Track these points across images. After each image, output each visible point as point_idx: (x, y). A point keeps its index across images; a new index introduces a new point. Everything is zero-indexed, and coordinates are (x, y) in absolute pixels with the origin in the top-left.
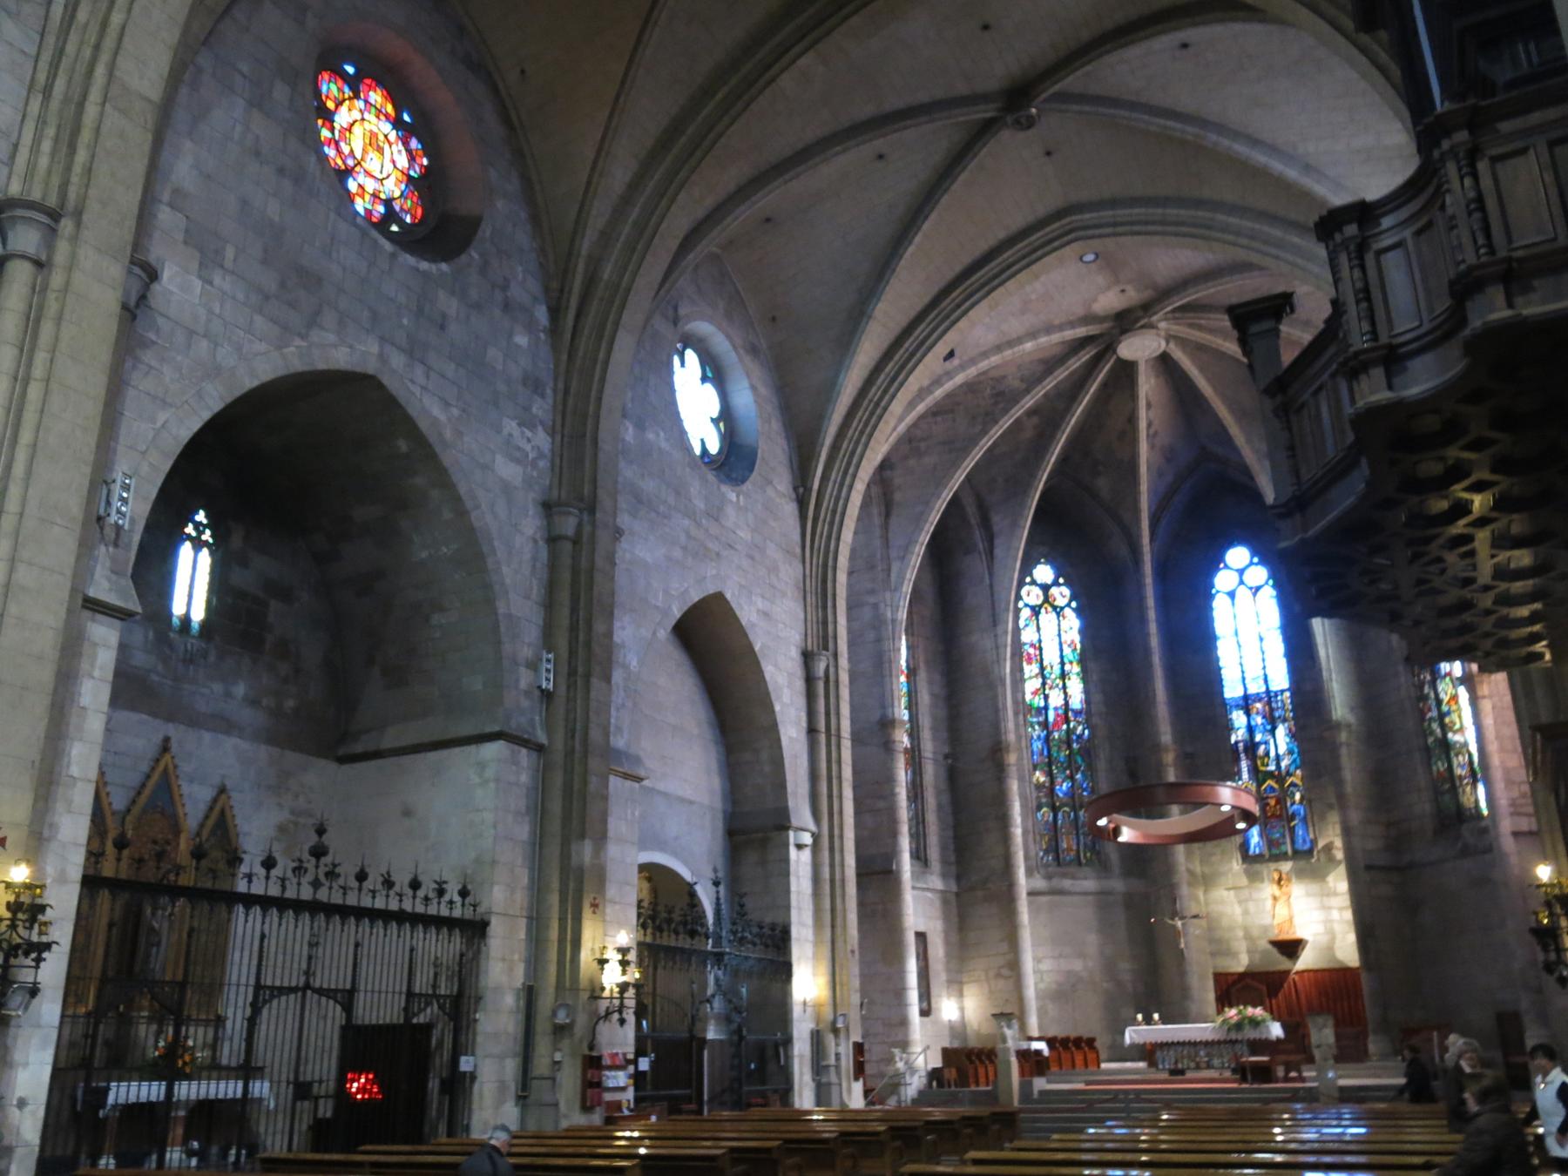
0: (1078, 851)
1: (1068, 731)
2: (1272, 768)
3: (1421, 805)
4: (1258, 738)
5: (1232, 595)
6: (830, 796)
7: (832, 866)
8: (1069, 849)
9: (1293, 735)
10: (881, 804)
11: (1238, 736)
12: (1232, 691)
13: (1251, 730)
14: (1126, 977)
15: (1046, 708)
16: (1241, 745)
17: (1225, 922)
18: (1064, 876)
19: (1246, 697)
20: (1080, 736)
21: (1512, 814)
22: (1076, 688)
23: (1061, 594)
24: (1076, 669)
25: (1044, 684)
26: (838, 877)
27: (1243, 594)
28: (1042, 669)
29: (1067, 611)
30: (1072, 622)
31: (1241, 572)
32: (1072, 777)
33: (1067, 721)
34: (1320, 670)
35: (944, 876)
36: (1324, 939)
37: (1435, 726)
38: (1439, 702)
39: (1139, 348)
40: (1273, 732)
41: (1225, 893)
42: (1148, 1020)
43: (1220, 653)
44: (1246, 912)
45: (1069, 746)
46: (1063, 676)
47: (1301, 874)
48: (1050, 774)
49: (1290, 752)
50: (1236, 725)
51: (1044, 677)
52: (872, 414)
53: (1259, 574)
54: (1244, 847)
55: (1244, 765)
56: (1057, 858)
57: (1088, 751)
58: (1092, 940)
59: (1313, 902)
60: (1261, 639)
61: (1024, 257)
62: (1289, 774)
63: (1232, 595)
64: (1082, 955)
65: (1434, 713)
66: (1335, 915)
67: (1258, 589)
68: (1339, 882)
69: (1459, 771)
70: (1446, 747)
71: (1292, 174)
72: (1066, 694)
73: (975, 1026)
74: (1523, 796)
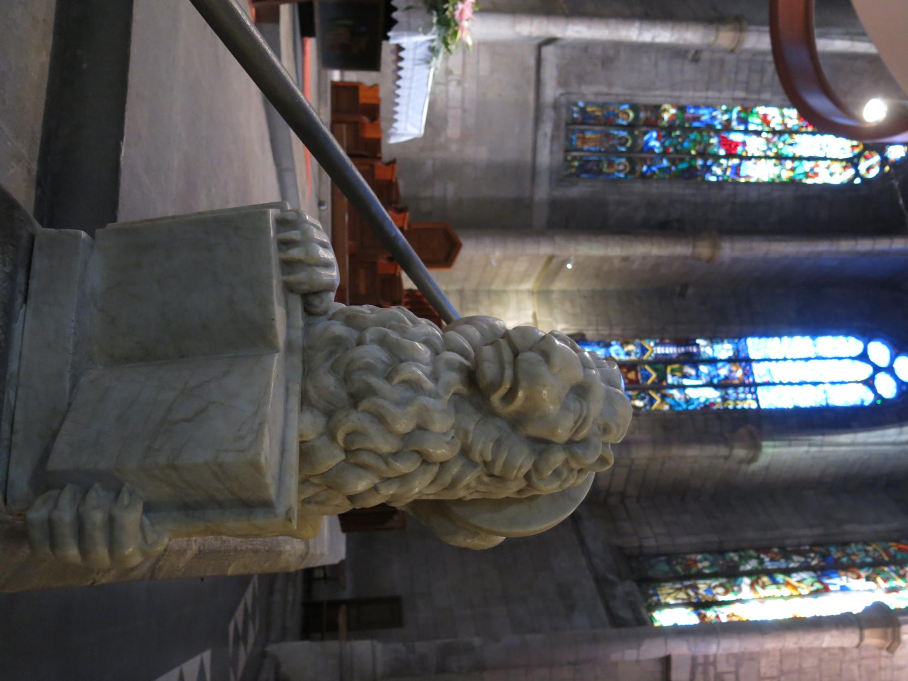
0: (581, 150)
1: (717, 157)
2: (670, 380)
3: (652, 536)
4: (704, 369)
5: (863, 357)
8: (584, 140)
9: (708, 407)
11: (705, 348)
12: (756, 346)
13: (713, 361)
14: (437, 191)
15: (746, 132)
16: (695, 350)
18: (556, 127)
19: (748, 361)
20: (708, 169)
21: (694, 659)
23: (870, 167)
24: (786, 175)
25: (774, 132)
27: (865, 371)
28: (791, 132)
29: (851, 172)
30: (839, 176)
31: (890, 370)
33: (728, 156)
34: (823, 434)
38: (788, 572)
40: (710, 384)
41: (530, 313)
43: (797, 339)
46: (780, 158)
48: (671, 127)
49: (688, 401)
50: (717, 347)
51: (780, 133)
55: (671, 350)
56: (574, 122)
57: (691, 174)
58: (480, 153)
60: (815, 384)
62: (664, 397)
64: (464, 138)
65: (769, 565)
69: (702, 586)
70: (731, 575)
72: (759, 158)
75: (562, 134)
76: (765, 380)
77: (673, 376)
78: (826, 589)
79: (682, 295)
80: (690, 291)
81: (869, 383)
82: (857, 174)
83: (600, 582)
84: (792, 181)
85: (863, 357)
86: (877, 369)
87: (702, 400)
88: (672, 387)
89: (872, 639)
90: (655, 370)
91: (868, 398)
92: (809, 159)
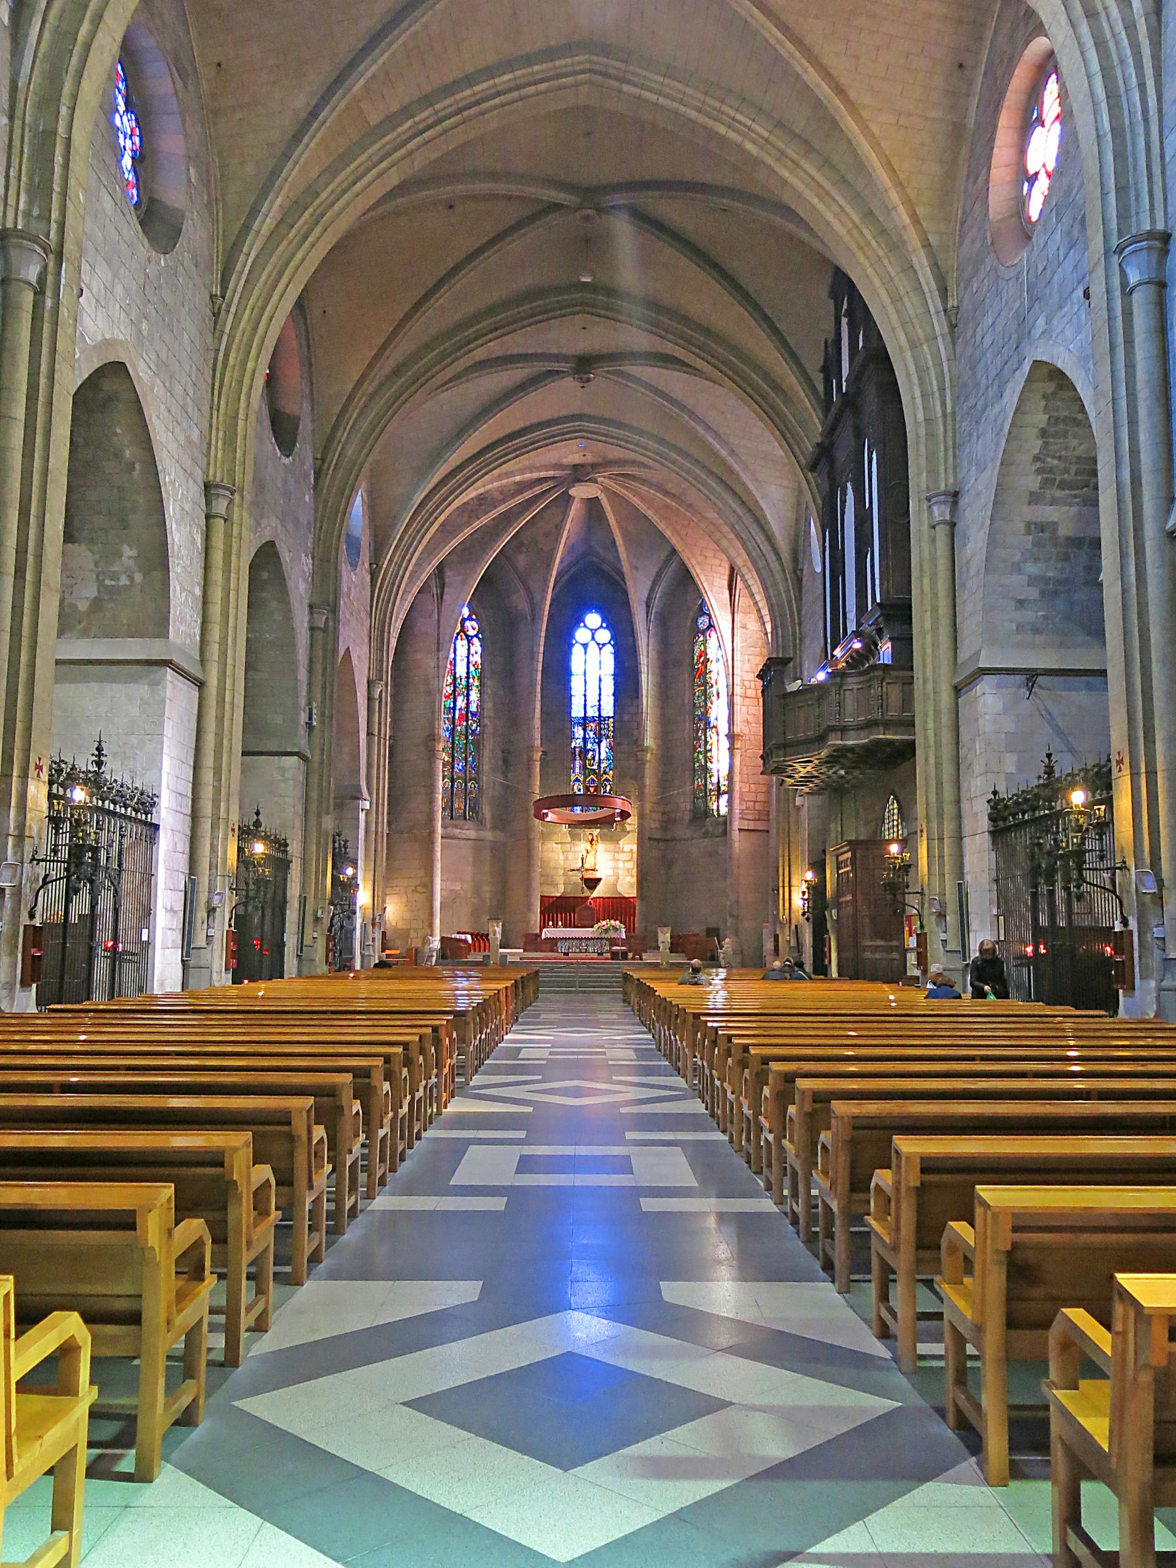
1: (467, 727)
2: (595, 767)
4: (589, 746)
5: (585, 646)
6: (378, 778)
7: (377, 823)
11: (577, 743)
12: (577, 712)
13: (585, 740)
14: (487, 895)
17: (552, 864)
18: (456, 827)
19: (585, 718)
22: (474, 695)
23: (472, 627)
24: (476, 683)
25: (454, 691)
27: (593, 647)
28: (455, 679)
29: (475, 640)
30: (477, 646)
31: (593, 631)
32: (466, 759)
36: (612, 879)
37: (701, 757)
38: (706, 742)
39: (580, 492)
40: (599, 744)
42: (555, 925)
43: (573, 685)
44: (566, 859)
45: (467, 738)
46: (468, 687)
47: (604, 837)
51: (455, 687)
52: (427, 520)
53: (604, 636)
55: (578, 763)
58: (469, 870)
59: (609, 856)
60: (600, 680)
61: (545, 439)
63: (585, 646)
64: (461, 881)
65: (702, 749)
66: (621, 864)
67: (604, 645)
68: (629, 845)
69: (710, 786)
70: (705, 770)
71: (724, 453)
73: (394, 924)
74: (747, 809)
75: (457, 822)
78: (715, 727)
81: (601, 646)
82: (476, 636)
83: (706, 835)
84: (479, 678)
88: (599, 766)
89: (738, 745)
91: (609, 649)
92: (468, 668)
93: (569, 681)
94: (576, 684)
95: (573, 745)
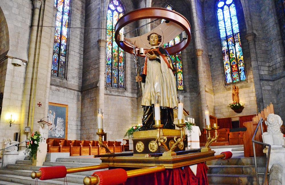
4: (230, 48)
5: (222, 8)
10: (97, 66)
11: (225, 48)
12: (223, 35)
13: (228, 46)
26: (34, 77)
27: (226, 7)
35: (132, 93)
50: (224, 45)
54: (226, 80)
60: (231, 19)
67: (230, 5)
76: (231, 32)
77: (233, 56)
79: (211, 56)
80: (210, 54)
81: (229, 6)
85: (222, 8)
86: (225, 4)
87: (239, 47)
88: (236, 56)
90: (232, 61)
93: (218, 24)
94: (221, 25)
95: (223, 49)
